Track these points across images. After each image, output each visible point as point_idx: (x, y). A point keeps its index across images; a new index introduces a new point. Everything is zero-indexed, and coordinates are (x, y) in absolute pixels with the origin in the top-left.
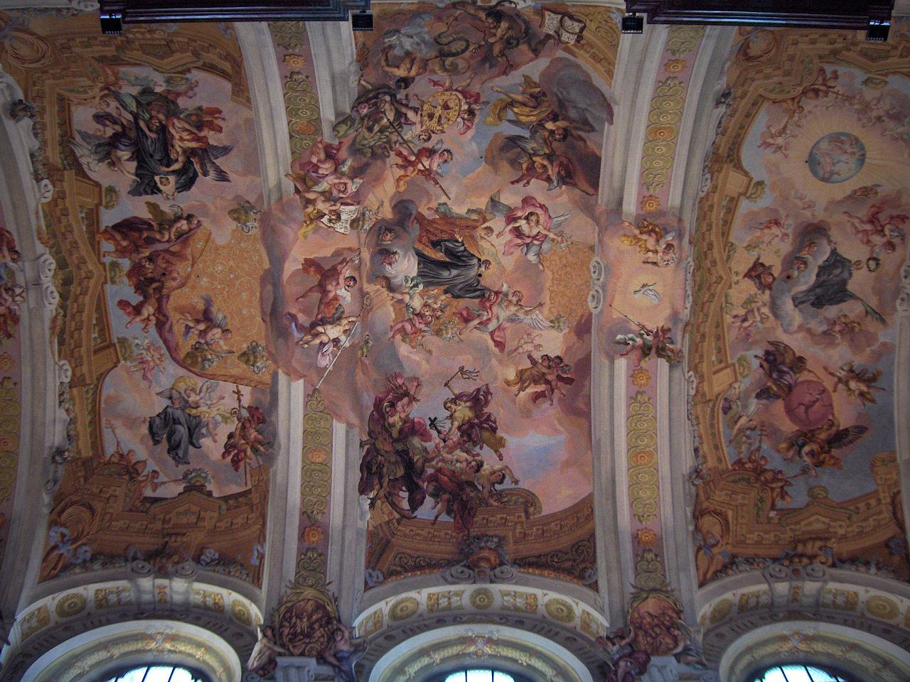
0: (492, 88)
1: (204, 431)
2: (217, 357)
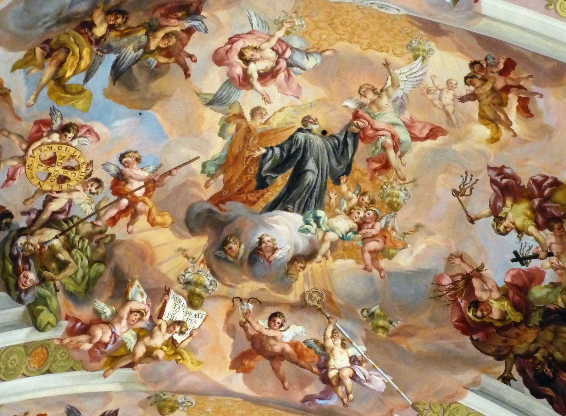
0: (28, 106)
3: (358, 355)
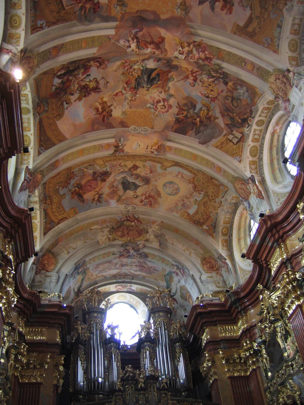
0: (216, 106)
3: (129, 49)
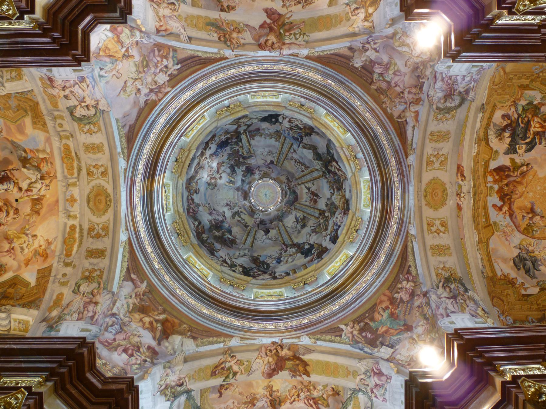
1: (540, 263)
2: (539, 229)
